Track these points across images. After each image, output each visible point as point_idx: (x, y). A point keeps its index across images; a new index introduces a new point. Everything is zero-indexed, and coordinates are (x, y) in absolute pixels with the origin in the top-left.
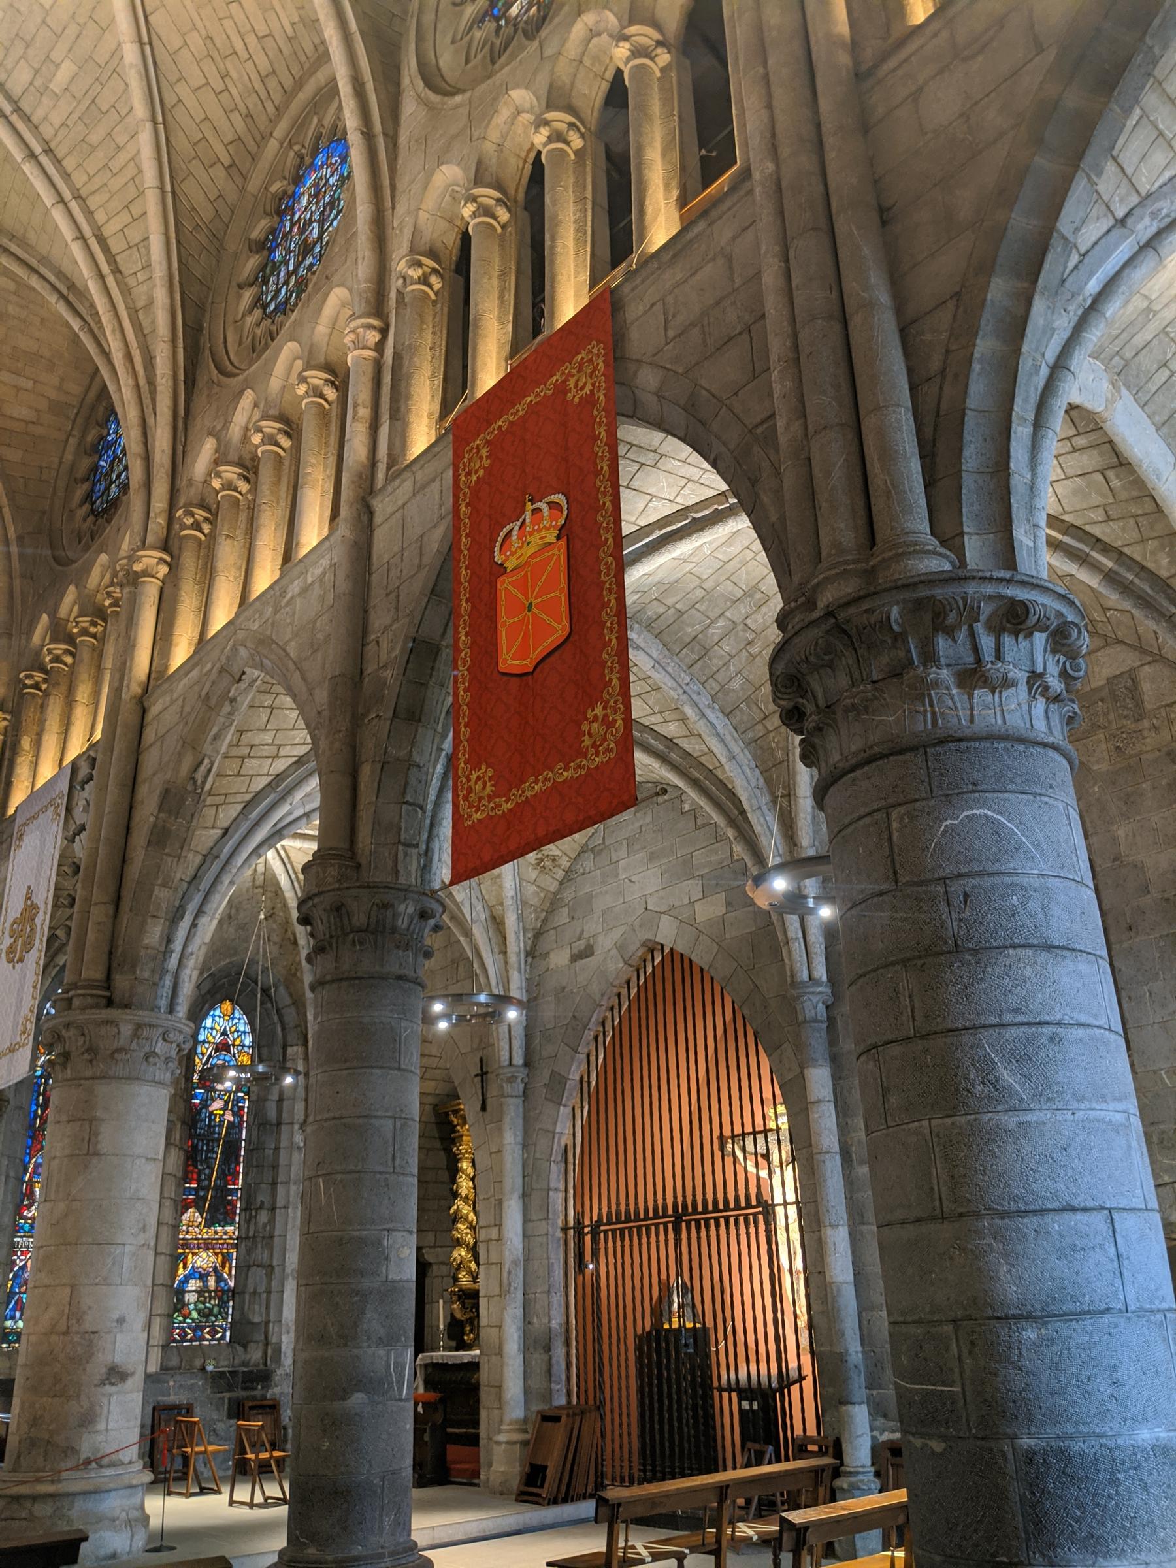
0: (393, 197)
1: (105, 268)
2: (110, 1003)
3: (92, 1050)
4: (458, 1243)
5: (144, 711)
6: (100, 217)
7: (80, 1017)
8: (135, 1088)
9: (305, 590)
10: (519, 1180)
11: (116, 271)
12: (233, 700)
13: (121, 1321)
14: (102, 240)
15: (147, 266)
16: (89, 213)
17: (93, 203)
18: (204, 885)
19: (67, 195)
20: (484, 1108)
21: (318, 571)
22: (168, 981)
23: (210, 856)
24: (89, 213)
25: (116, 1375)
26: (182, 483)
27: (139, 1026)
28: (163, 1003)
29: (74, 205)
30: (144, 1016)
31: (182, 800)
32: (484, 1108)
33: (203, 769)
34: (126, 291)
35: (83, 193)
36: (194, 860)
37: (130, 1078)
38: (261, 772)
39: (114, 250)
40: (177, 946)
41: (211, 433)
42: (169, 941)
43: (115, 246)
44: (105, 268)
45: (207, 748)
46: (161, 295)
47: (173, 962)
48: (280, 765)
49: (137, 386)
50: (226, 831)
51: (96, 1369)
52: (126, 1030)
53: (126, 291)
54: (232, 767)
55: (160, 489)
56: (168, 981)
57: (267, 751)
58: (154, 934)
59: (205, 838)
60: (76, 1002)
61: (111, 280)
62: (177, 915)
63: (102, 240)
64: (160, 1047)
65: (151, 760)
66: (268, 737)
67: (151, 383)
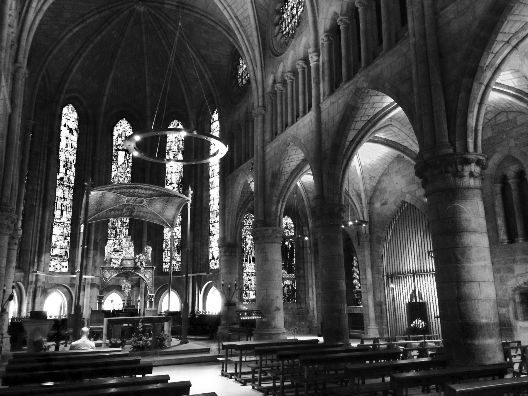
0: (317, 6)
1: (239, 26)
2: (266, 225)
3: (263, 236)
4: (355, 278)
5: (264, 151)
6: (235, 10)
7: (259, 229)
8: (274, 244)
9: (304, 126)
10: (370, 264)
11: (242, 26)
12: (287, 150)
13: (277, 297)
14: (236, 17)
15: (250, 23)
16: (232, 10)
17: (233, 7)
18: (284, 195)
19: (226, 6)
20: (359, 244)
21: (307, 121)
22: (278, 218)
23: (284, 187)
24: (232, 10)
25: (278, 309)
26: (265, 86)
27: (273, 231)
28: (277, 224)
29: (228, 9)
30: (274, 228)
31: (277, 175)
32: (359, 244)
33: (281, 167)
34: (245, 31)
35: (230, 4)
36: (280, 188)
37: (272, 243)
38: (293, 164)
39: (240, 20)
40: (279, 210)
41: (272, 73)
42: (277, 208)
43: (240, 18)
44: (239, 26)
45: (282, 162)
46: (255, 33)
47: (279, 213)
48: (298, 162)
49: (251, 59)
50: (287, 180)
51: (274, 308)
52: (270, 231)
53: (245, 31)
54: (288, 164)
55: (260, 90)
56: (278, 218)
57: (295, 159)
58: (274, 208)
59: (283, 182)
60: (258, 225)
61: (240, 29)
62: (278, 202)
63: (236, 17)
64: (278, 235)
65: (268, 164)
66: (295, 156)
67: (254, 58)
